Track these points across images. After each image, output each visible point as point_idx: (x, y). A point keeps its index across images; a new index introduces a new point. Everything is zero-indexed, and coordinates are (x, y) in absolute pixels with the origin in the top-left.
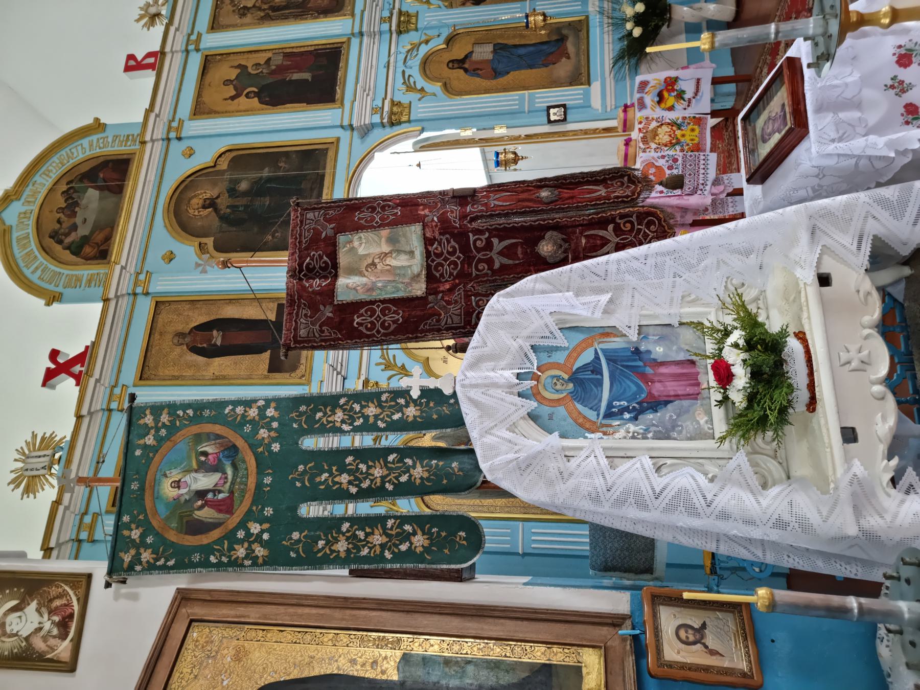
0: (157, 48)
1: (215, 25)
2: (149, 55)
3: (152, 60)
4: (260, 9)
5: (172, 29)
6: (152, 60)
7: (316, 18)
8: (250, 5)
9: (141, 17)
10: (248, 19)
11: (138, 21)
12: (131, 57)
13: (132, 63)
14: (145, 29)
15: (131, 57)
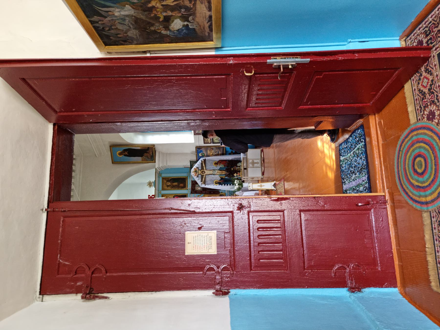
0: (154, 194)
1: (163, 189)
2: (153, 195)
3: (153, 197)
4: (171, 186)
5: (156, 190)
6: (153, 197)
7: (181, 189)
8: (169, 185)
9: (148, 185)
10: (169, 188)
11: (147, 186)
12: (149, 196)
13: (150, 197)
14: (149, 188)
15: (149, 196)
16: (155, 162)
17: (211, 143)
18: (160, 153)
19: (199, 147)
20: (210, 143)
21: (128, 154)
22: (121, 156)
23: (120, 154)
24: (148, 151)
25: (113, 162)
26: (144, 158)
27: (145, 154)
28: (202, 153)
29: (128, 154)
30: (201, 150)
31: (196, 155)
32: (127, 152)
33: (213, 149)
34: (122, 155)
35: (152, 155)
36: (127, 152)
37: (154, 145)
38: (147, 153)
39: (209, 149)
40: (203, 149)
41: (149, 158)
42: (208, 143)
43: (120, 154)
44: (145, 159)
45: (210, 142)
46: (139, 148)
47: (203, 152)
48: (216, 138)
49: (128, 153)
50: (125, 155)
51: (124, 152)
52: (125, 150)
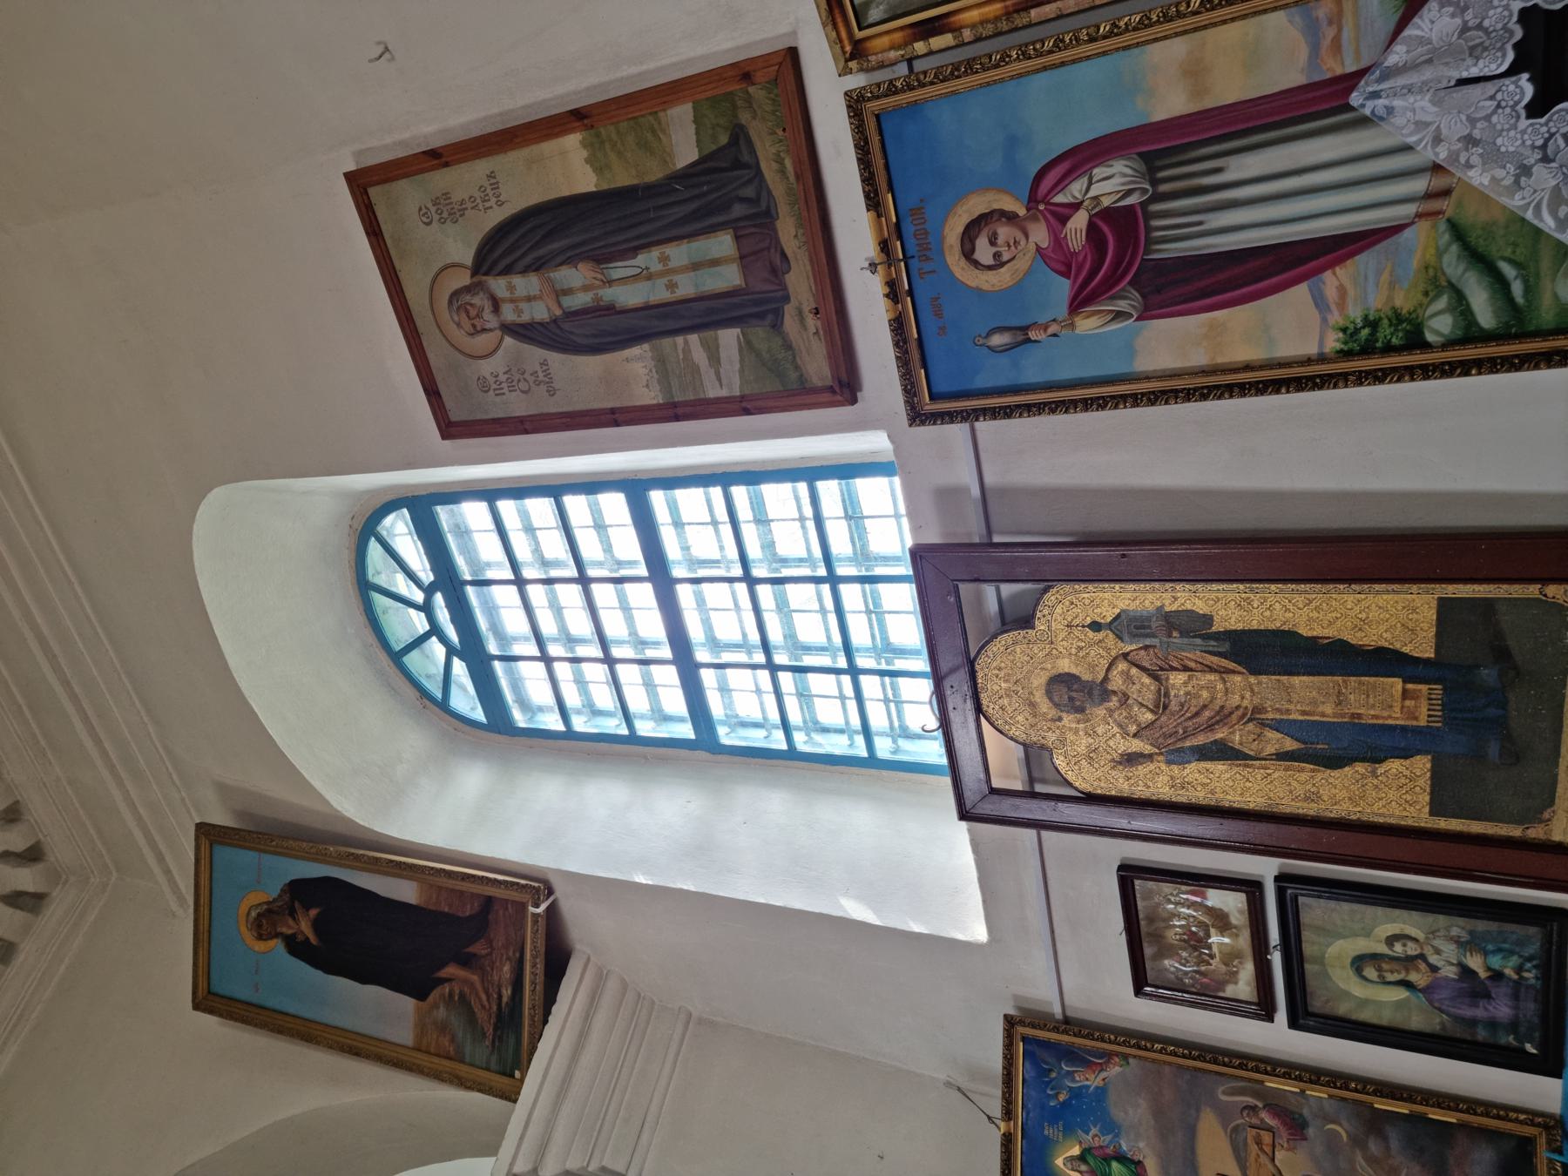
16: (511, 1096)
17: (1265, 1010)
18: (612, 986)
19: (1069, 1023)
20: (1234, 1008)
21: (313, 939)
22: (260, 946)
23: (265, 922)
24: (478, 948)
25: (207, 999)
26: (441, 1013)
27: (451, 970)
28: (1094, 1136)
29: (313, 939)
30: (1092, 1080)
31: (1007, 1140)
32: (313, 912)
33: (1296, 1126)
34: (277, 935)
35: (507, 993)
36: (313, 912)
37: (540, 885)
38: (467, 961)
39: (1224, 1114)
40: (1114, 1070)
41: (484, 1035)
42: (1207, 996)
43: (265, 922)
44: (443, 1028)
45: (1243, 986)
46: (406, 891)
47: (1111, 1127)
48: (1363, 945)
49: (316, 925)
50: (297, 948)
51: (292, 913)
52: (300, 891)
